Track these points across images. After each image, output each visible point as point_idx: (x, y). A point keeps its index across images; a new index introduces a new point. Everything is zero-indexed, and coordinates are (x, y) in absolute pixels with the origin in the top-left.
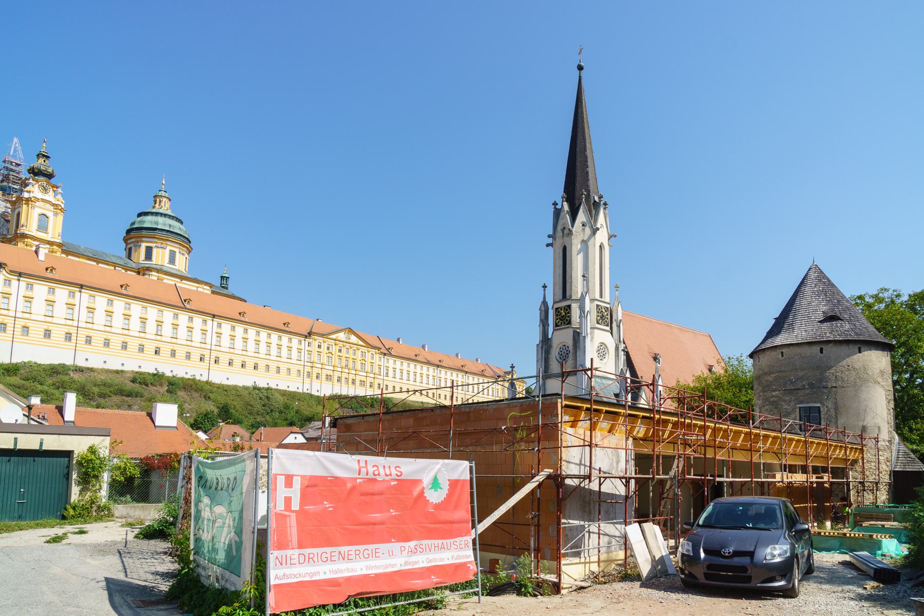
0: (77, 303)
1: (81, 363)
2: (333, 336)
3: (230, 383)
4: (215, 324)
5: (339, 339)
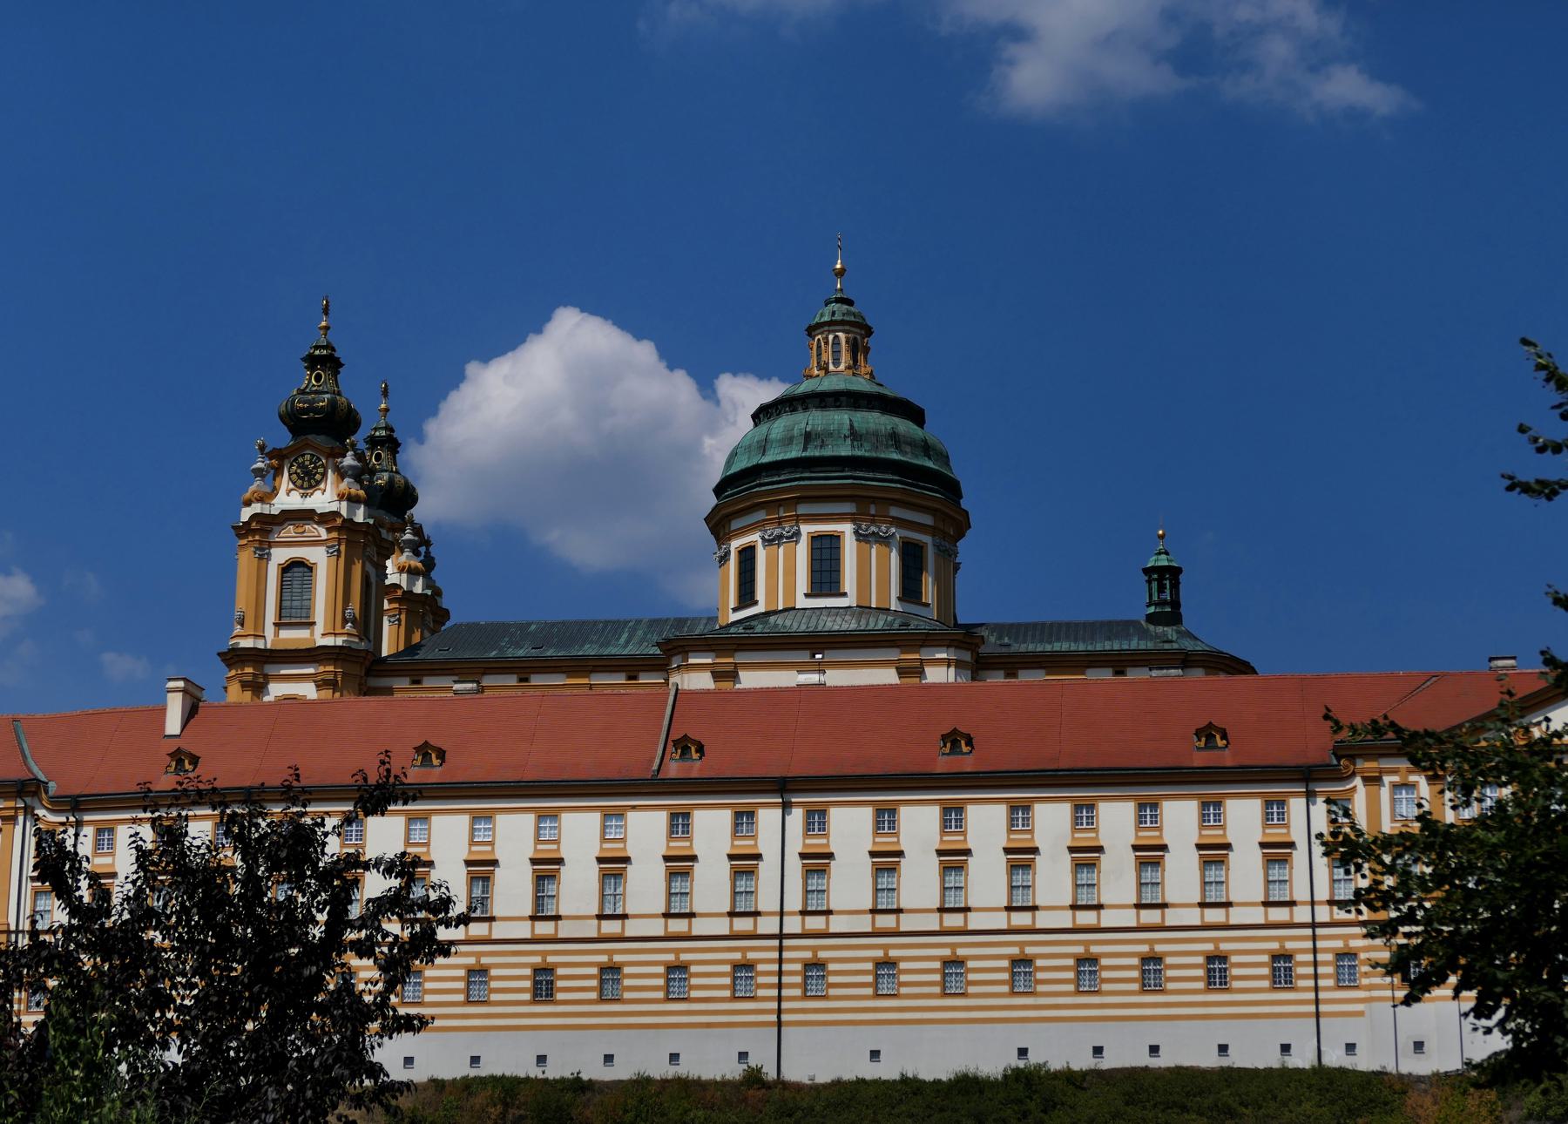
3: (887, 1070)
4: (797, 816)
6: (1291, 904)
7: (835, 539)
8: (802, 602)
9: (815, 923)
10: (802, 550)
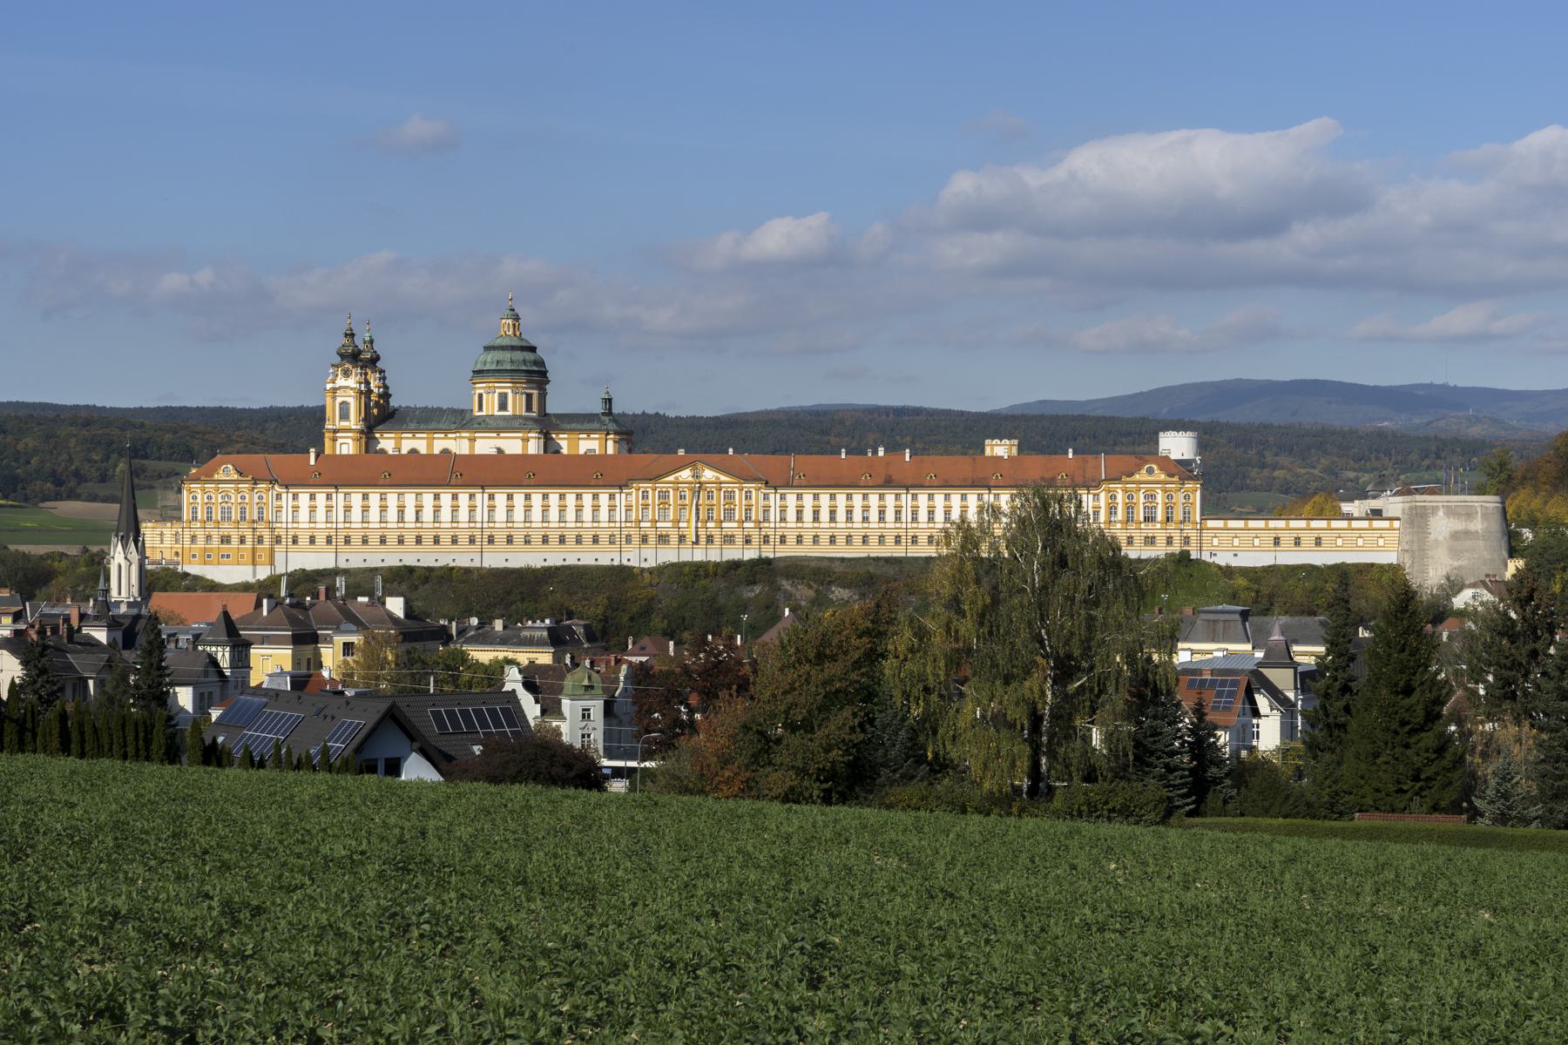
2: (671, 478)
7: (506, 394)
8: (496, 413)
10: (496, 395)
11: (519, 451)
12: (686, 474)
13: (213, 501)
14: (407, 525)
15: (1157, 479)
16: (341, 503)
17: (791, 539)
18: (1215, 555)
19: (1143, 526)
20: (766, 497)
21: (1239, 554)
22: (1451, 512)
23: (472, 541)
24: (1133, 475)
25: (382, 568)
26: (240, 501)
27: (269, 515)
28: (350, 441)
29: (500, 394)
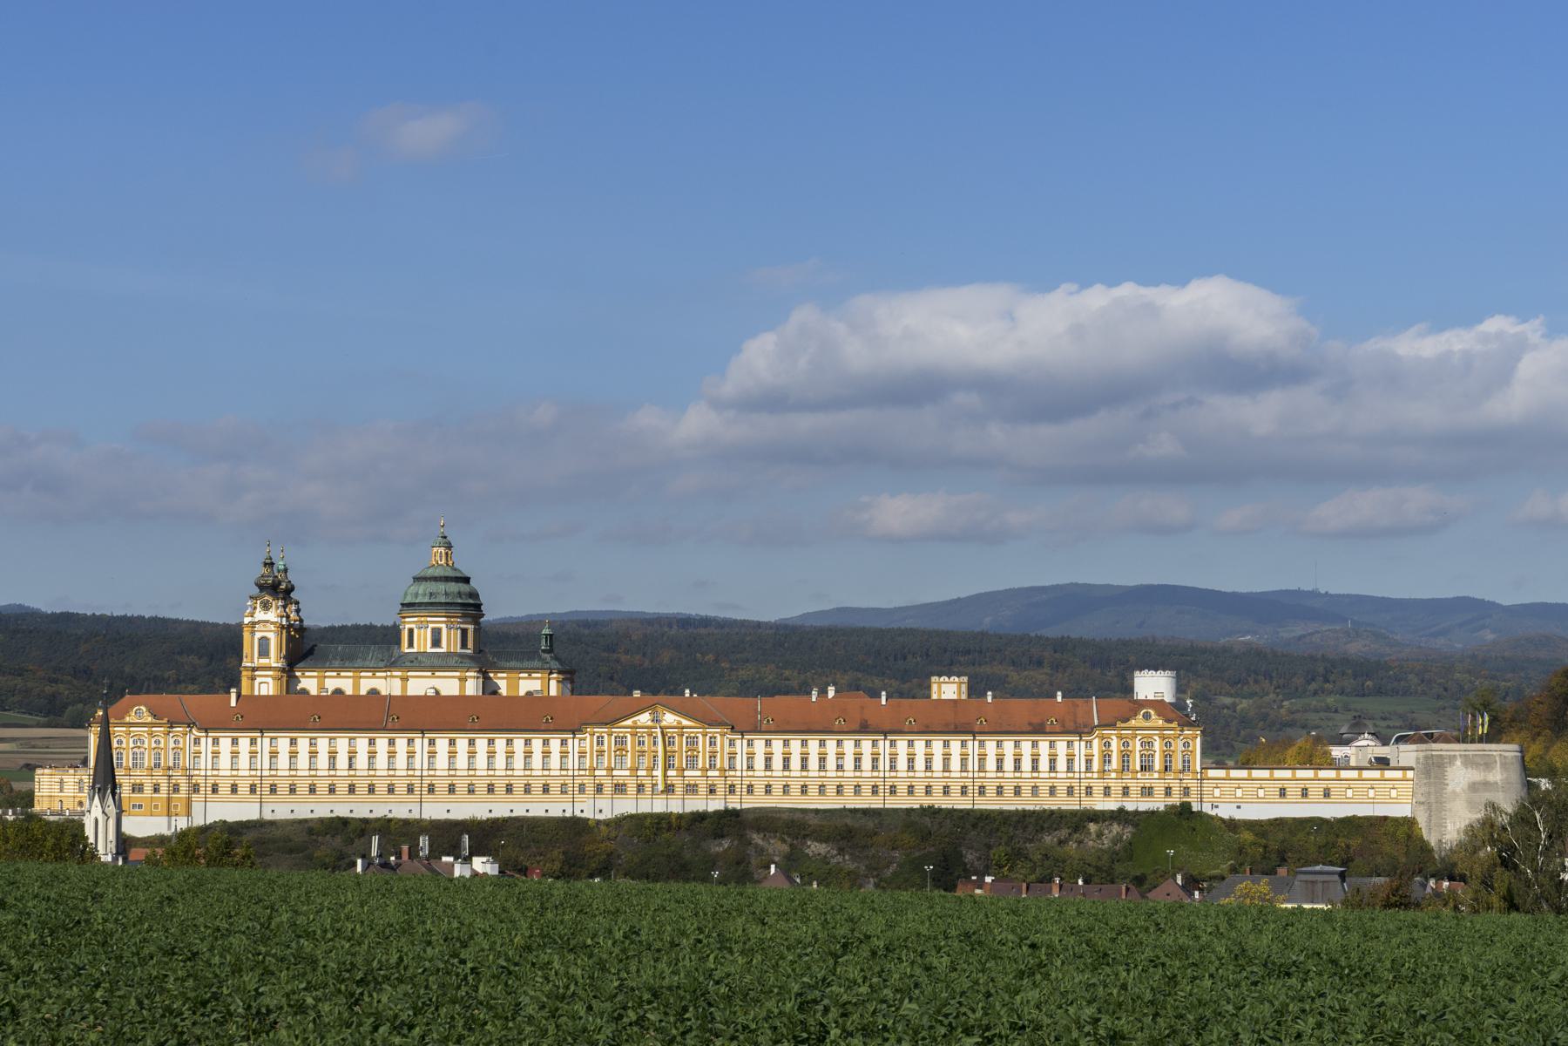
0: (259, 751)
1: (268, 816)
2: (629, 722)
5: (639, 723)
6: (568, 770)
9: (432, 773)
10: (429, 630)
11: (456, 692)
12: (644, 718)
13: (124, 745)
14: (339, 773)
15: (1155, 725)
16: (267, 748)
17: (759, 789)
18: (1217, 807)
19: (1139, 775)
20: (732, 743)
21: (1242, 805)
22: (1468, 762)
23: (410, 790)
24: (1127, 720)
25: (312, 820)
26: (154, 745)
27: (186, 761)
28: (269, 680)
29: (433, 629)
